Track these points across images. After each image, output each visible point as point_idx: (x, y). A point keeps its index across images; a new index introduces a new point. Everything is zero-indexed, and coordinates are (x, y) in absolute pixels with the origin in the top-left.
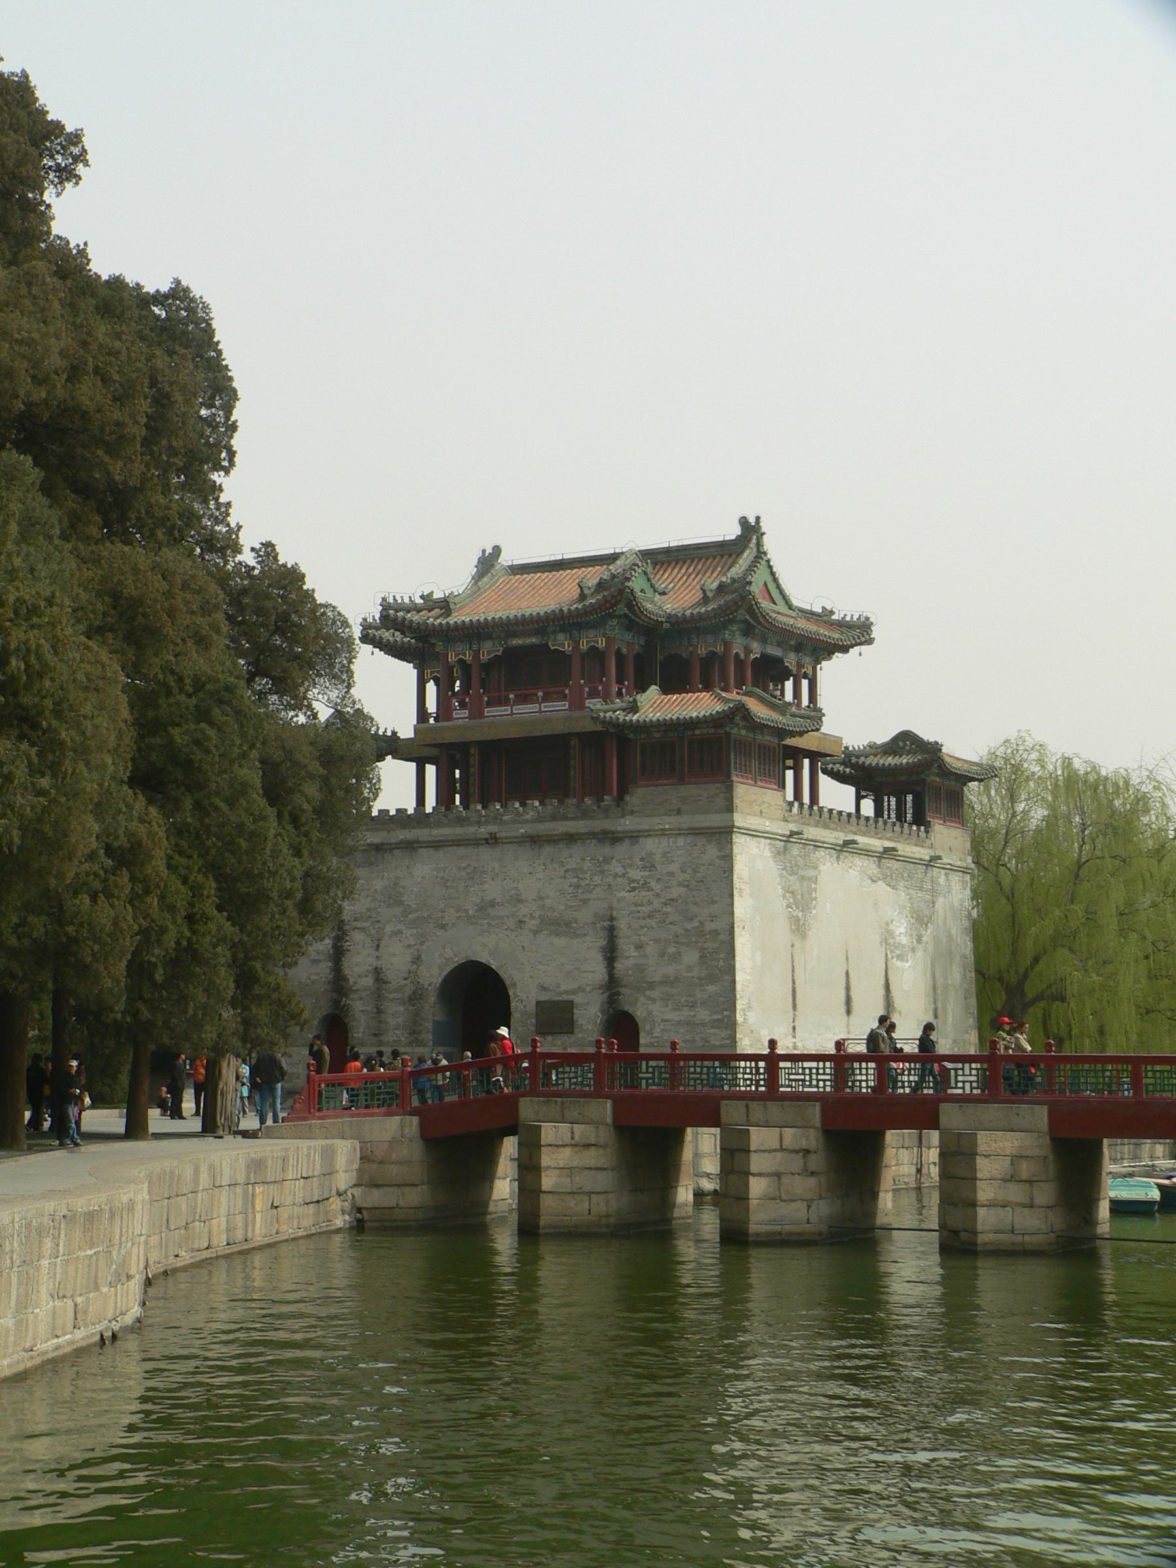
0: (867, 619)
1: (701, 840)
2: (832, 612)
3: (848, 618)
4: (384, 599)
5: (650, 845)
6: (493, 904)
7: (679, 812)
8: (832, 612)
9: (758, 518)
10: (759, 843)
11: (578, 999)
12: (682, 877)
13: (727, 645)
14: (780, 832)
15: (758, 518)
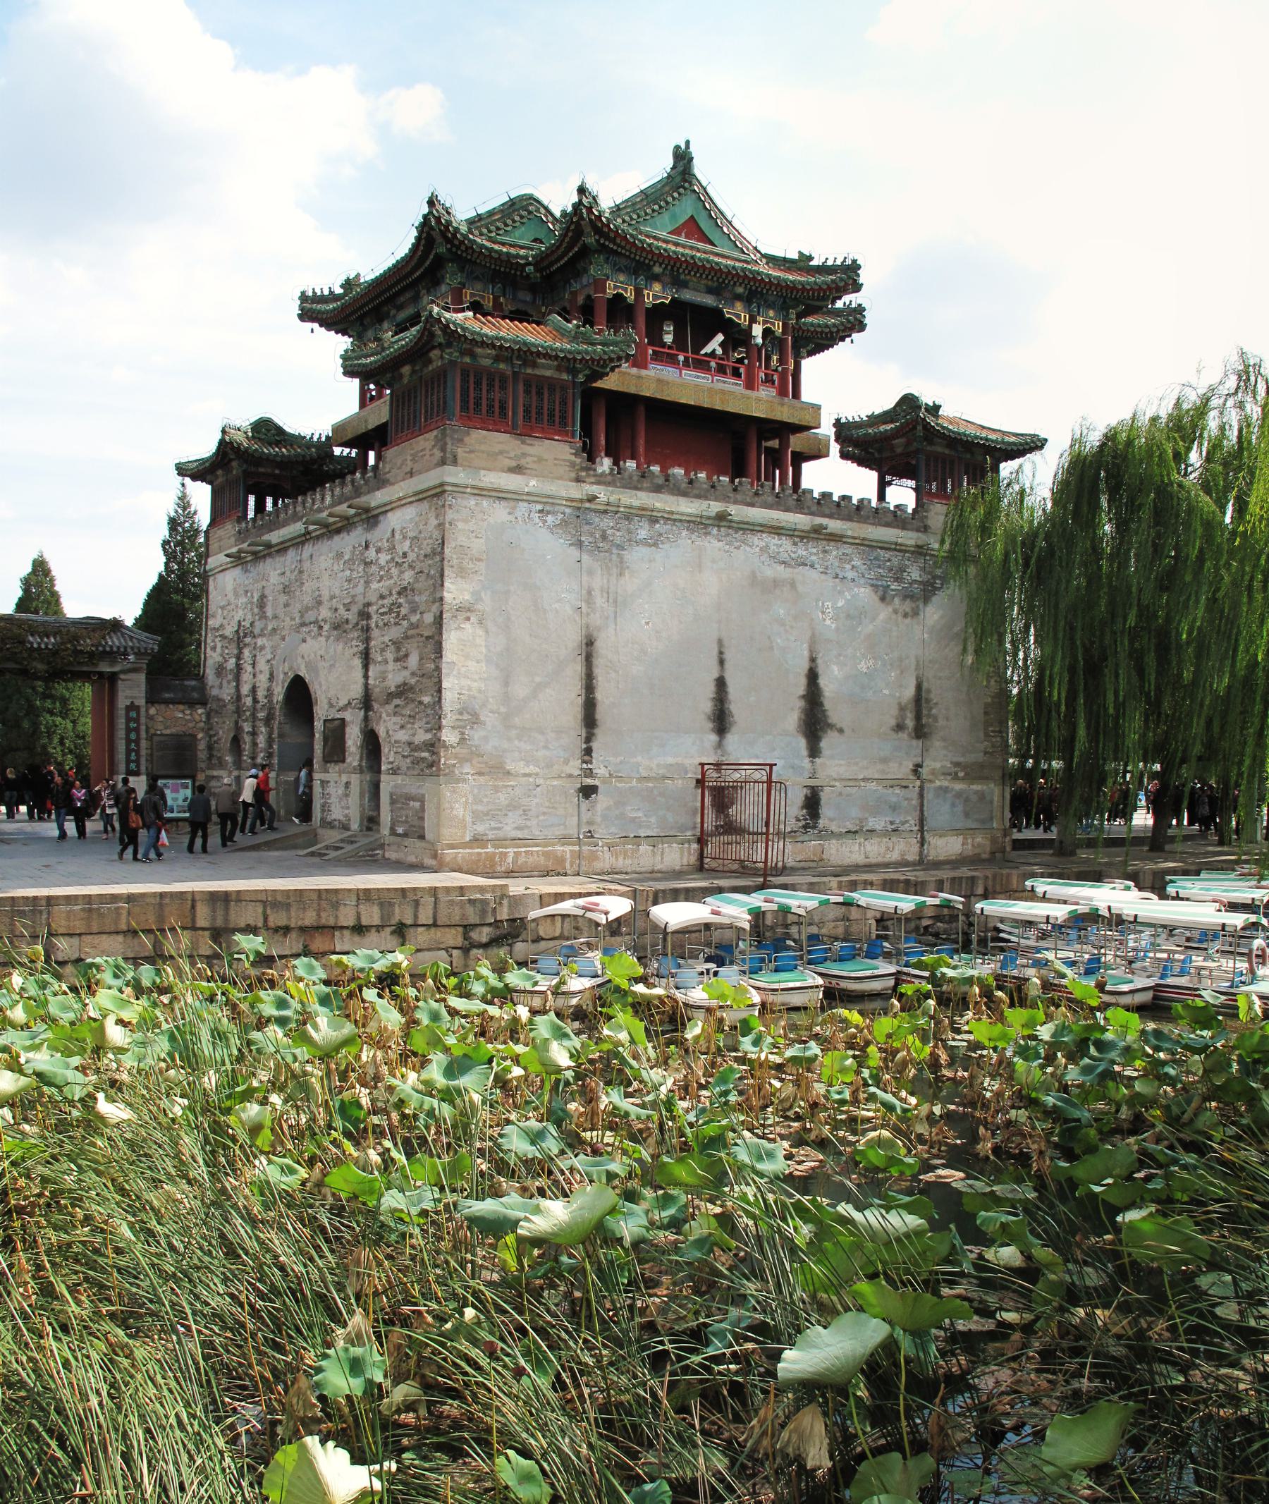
0: (854, 261)
1: (425, 505)
2: (811, 258)
3: (830, 263)
4: (303, 293)
5: (395, 520)
6: (308, 609)
7: (411, 474)
8: (811, 258)
9: (688, 143)
10: (514, 508)
11: (347, 715)
12: (412, 556)
13: (600, 285)
14: (564, 494)
15: (688, 143)
